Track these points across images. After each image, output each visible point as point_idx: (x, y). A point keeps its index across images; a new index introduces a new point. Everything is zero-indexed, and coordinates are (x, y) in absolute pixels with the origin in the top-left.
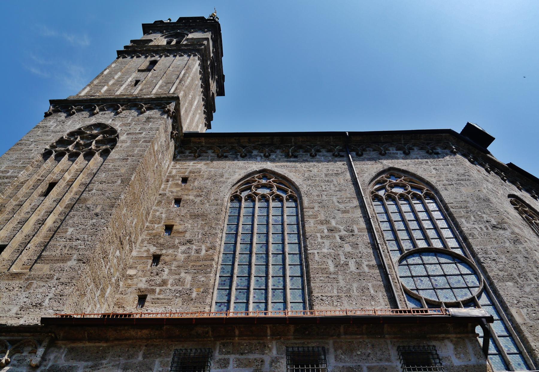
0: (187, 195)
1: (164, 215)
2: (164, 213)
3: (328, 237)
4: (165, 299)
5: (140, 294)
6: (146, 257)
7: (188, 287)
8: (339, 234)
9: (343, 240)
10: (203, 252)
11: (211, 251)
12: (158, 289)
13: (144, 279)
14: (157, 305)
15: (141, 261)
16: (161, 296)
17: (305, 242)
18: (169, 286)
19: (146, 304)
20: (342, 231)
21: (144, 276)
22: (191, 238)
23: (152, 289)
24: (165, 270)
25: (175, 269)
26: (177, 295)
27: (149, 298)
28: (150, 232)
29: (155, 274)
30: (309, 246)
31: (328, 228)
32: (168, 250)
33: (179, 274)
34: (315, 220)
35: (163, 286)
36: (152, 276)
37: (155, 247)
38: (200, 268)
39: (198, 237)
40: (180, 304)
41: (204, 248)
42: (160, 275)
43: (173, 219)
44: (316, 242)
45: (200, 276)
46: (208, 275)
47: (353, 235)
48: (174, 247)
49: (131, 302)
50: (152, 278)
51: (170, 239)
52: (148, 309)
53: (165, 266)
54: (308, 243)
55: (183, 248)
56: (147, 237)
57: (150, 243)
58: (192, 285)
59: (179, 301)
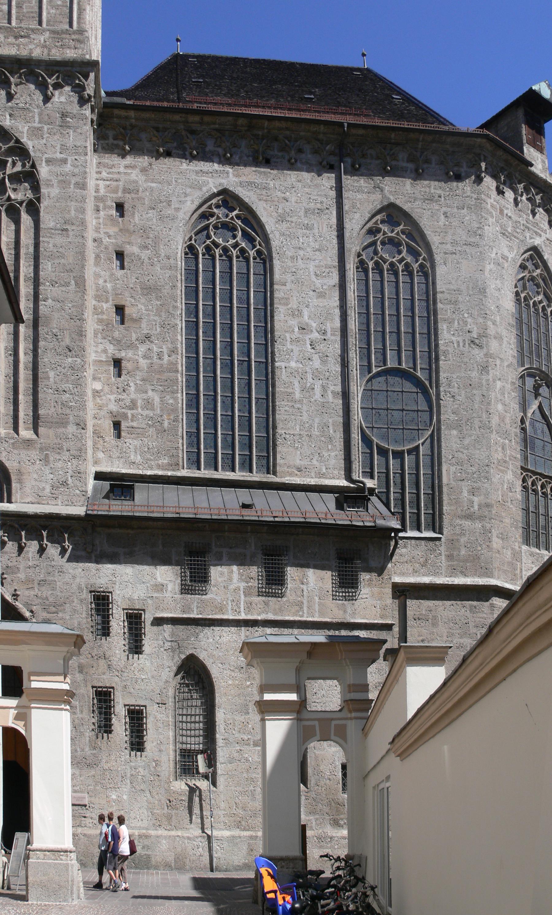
0: (129, 243)
1: (109, 285)
2: (108, 281)
3: (297, 340)
4: (139, 428)
5: (113, 420)
6: (106, 361)
7: (158, 412)
8: (310, 337)
9: (313, 348)
10: (166, 358)
11: (174, 356)
12: (129, 413)
13: (112, 397)
14: (133, 435)
15: (102, 368)
16: (135, 424)
17: (273, 346)
18: (140, 409)
19: (123, 434)
20: (314, 331)
21: (112, 393)
22: (149, 332)
23: (124, 413)
24: (131, 385)
25: (141, 383)
26: (150, 422)
27: (124, 425)
28: (100, 317)
29: (122, 390)
30: (277, 355)
31: (300, 325)
32: (127, 351)
33: (146, 392)
34: (286, 307)
35: (133, 409)
36: (120, 394)
37: (112, 346)
38: (166, 383)
39: (156, 330)
40: (155, 437)
41: (165, 350)
42: (127, 392)
43: (121, 294)
44: (285, 349)
45: (168, 397)
46: (176, 395)
47: (325, 340)
48: (131, 346)
49: (107, 431)
50: (120, 396)
51: (127, 332)
52: (126, 441)
53: (129, 378)
54: (276, 350)
55: (142, 349)
56: (99, 327)
57: (105, 338)
58: (162, 410)
59: (152, 431)
